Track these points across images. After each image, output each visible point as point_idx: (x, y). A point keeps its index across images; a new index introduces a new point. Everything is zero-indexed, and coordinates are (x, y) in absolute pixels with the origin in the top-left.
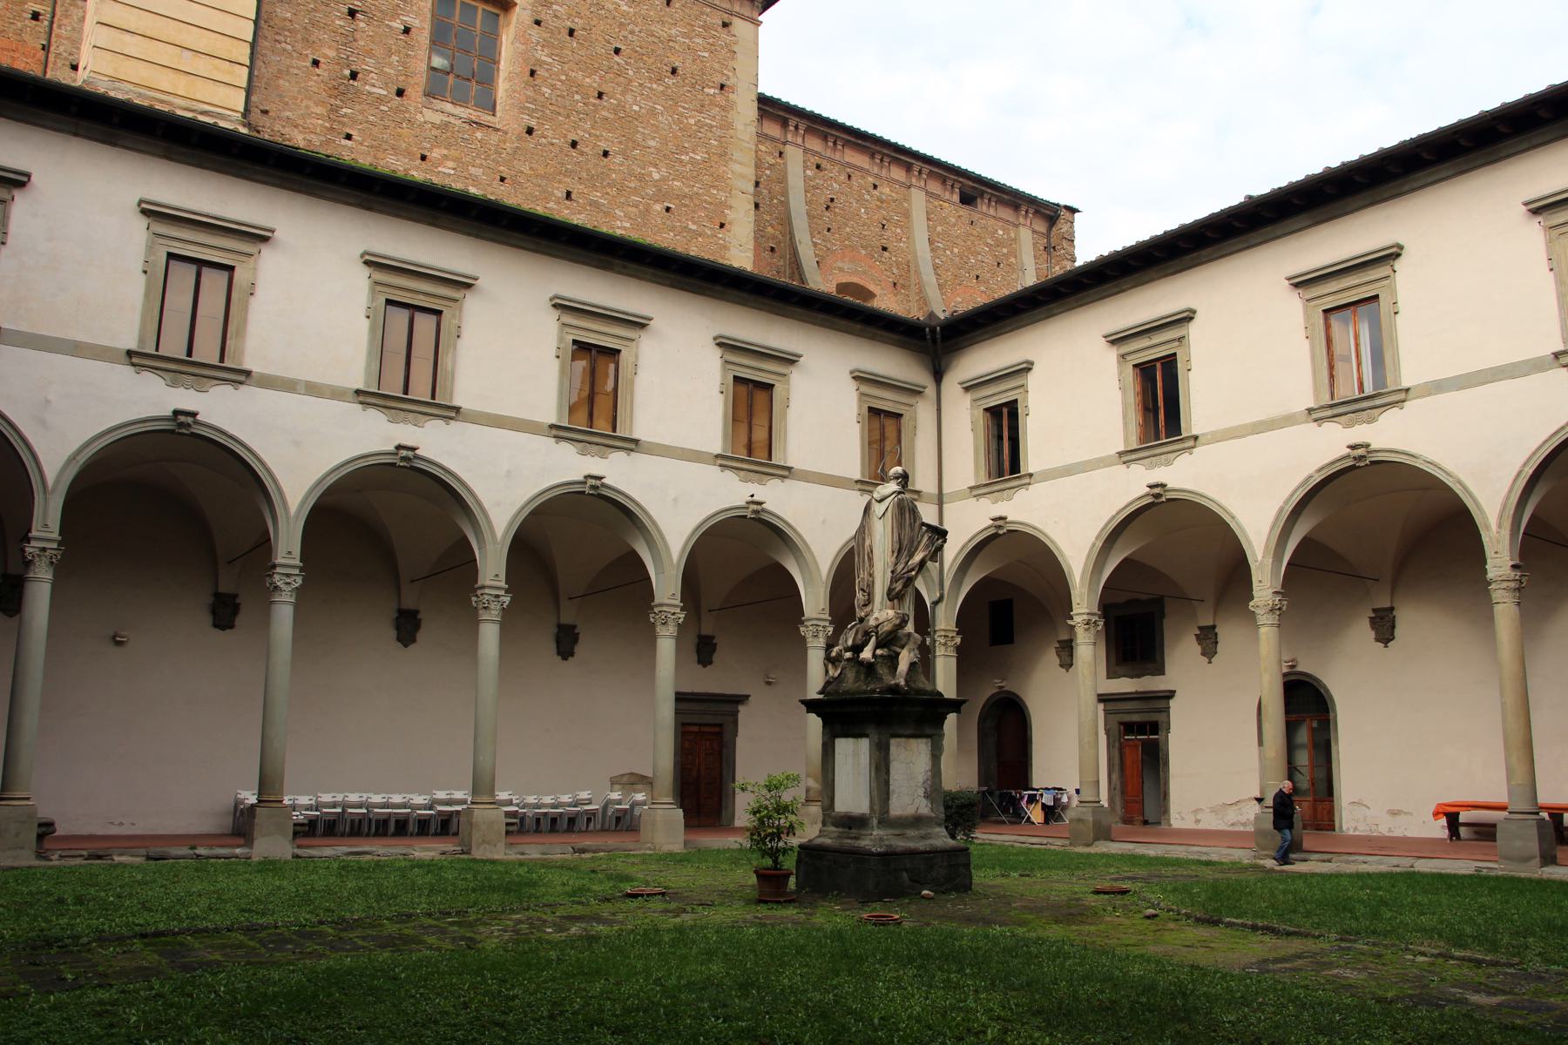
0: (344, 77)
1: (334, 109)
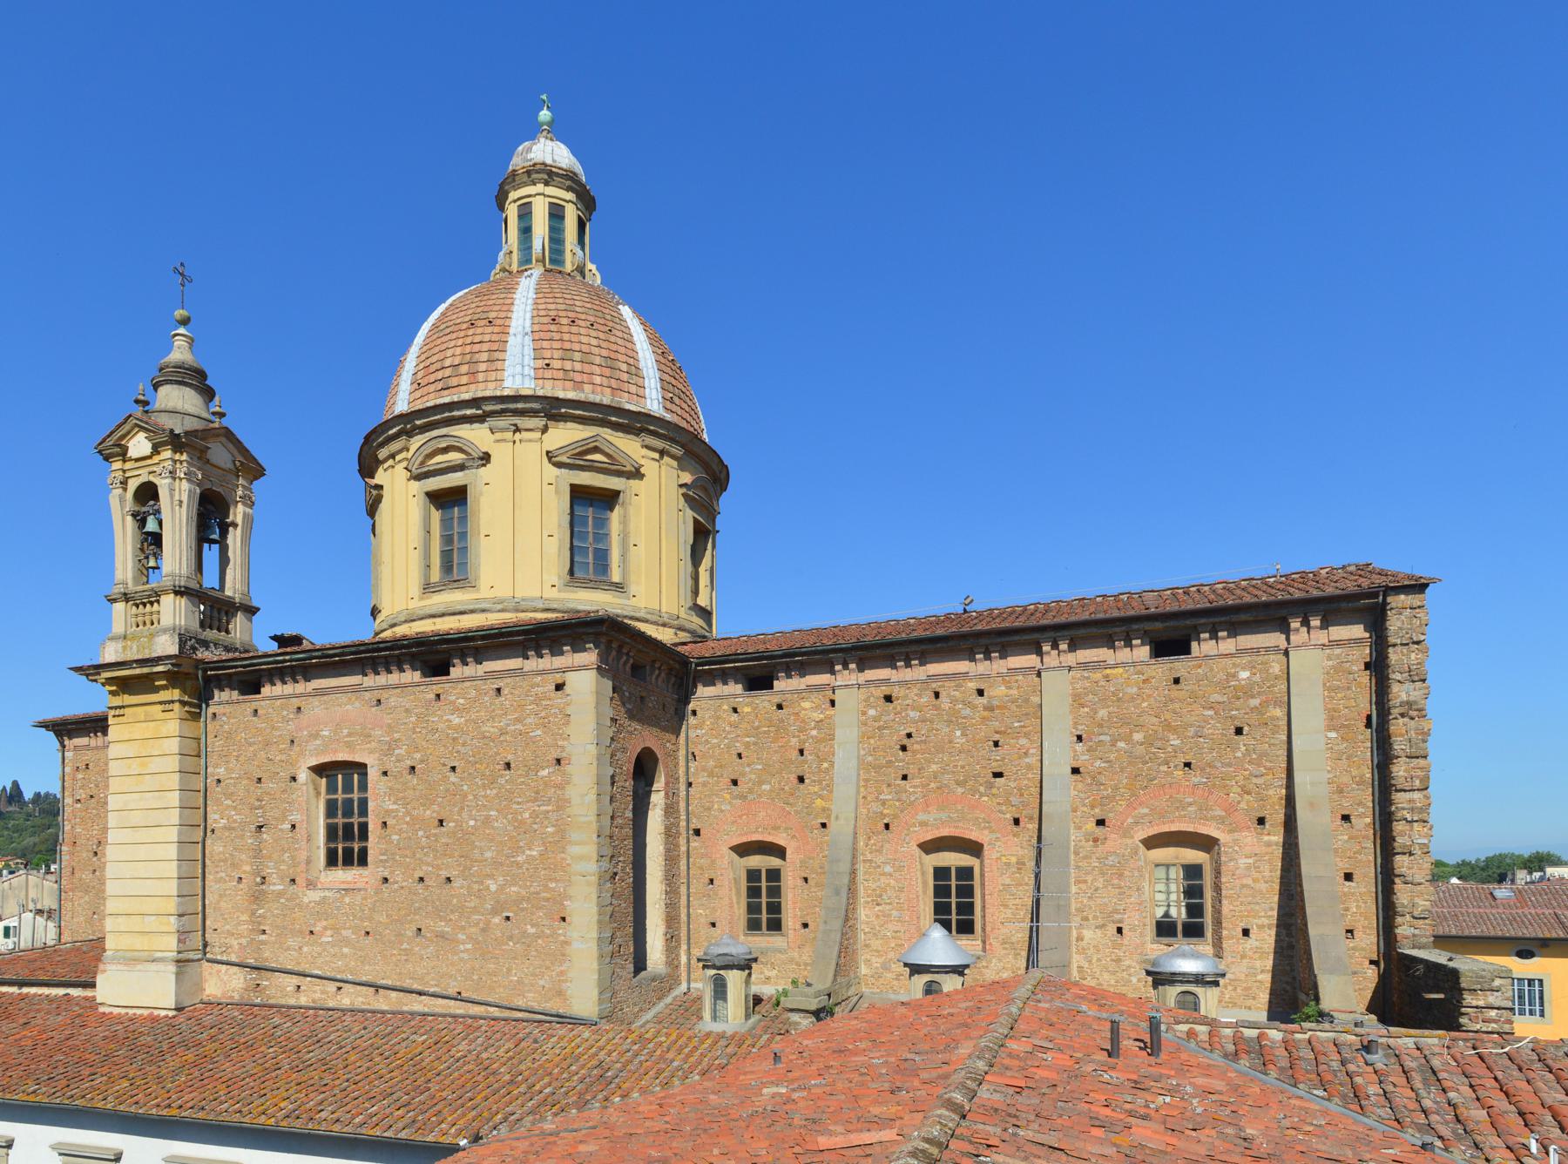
0: (257, 884)
1: (253, 913)
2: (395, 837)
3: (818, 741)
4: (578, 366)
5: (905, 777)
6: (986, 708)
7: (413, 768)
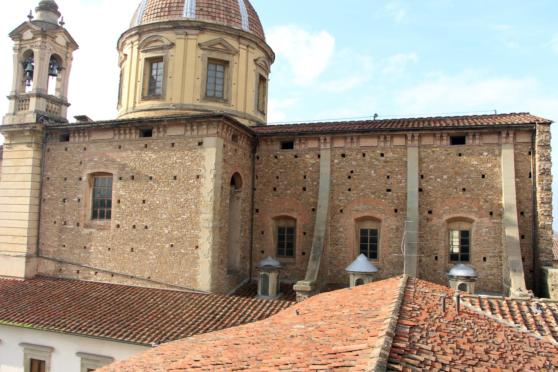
2: (123, 207)
3: (312, 172)
4: (214, 10)
5: (349, 190)
6: (385, 162)
7: (133, 177)
